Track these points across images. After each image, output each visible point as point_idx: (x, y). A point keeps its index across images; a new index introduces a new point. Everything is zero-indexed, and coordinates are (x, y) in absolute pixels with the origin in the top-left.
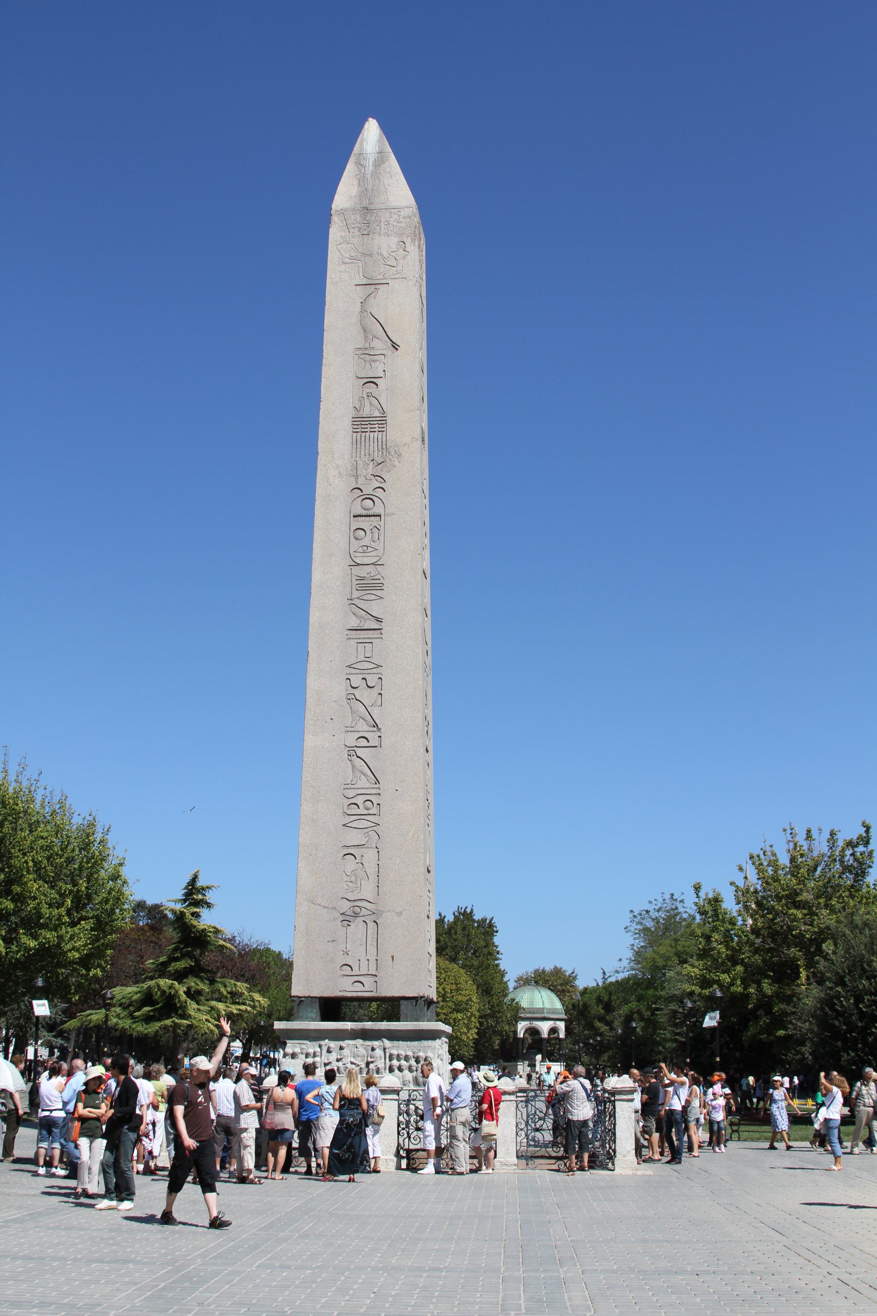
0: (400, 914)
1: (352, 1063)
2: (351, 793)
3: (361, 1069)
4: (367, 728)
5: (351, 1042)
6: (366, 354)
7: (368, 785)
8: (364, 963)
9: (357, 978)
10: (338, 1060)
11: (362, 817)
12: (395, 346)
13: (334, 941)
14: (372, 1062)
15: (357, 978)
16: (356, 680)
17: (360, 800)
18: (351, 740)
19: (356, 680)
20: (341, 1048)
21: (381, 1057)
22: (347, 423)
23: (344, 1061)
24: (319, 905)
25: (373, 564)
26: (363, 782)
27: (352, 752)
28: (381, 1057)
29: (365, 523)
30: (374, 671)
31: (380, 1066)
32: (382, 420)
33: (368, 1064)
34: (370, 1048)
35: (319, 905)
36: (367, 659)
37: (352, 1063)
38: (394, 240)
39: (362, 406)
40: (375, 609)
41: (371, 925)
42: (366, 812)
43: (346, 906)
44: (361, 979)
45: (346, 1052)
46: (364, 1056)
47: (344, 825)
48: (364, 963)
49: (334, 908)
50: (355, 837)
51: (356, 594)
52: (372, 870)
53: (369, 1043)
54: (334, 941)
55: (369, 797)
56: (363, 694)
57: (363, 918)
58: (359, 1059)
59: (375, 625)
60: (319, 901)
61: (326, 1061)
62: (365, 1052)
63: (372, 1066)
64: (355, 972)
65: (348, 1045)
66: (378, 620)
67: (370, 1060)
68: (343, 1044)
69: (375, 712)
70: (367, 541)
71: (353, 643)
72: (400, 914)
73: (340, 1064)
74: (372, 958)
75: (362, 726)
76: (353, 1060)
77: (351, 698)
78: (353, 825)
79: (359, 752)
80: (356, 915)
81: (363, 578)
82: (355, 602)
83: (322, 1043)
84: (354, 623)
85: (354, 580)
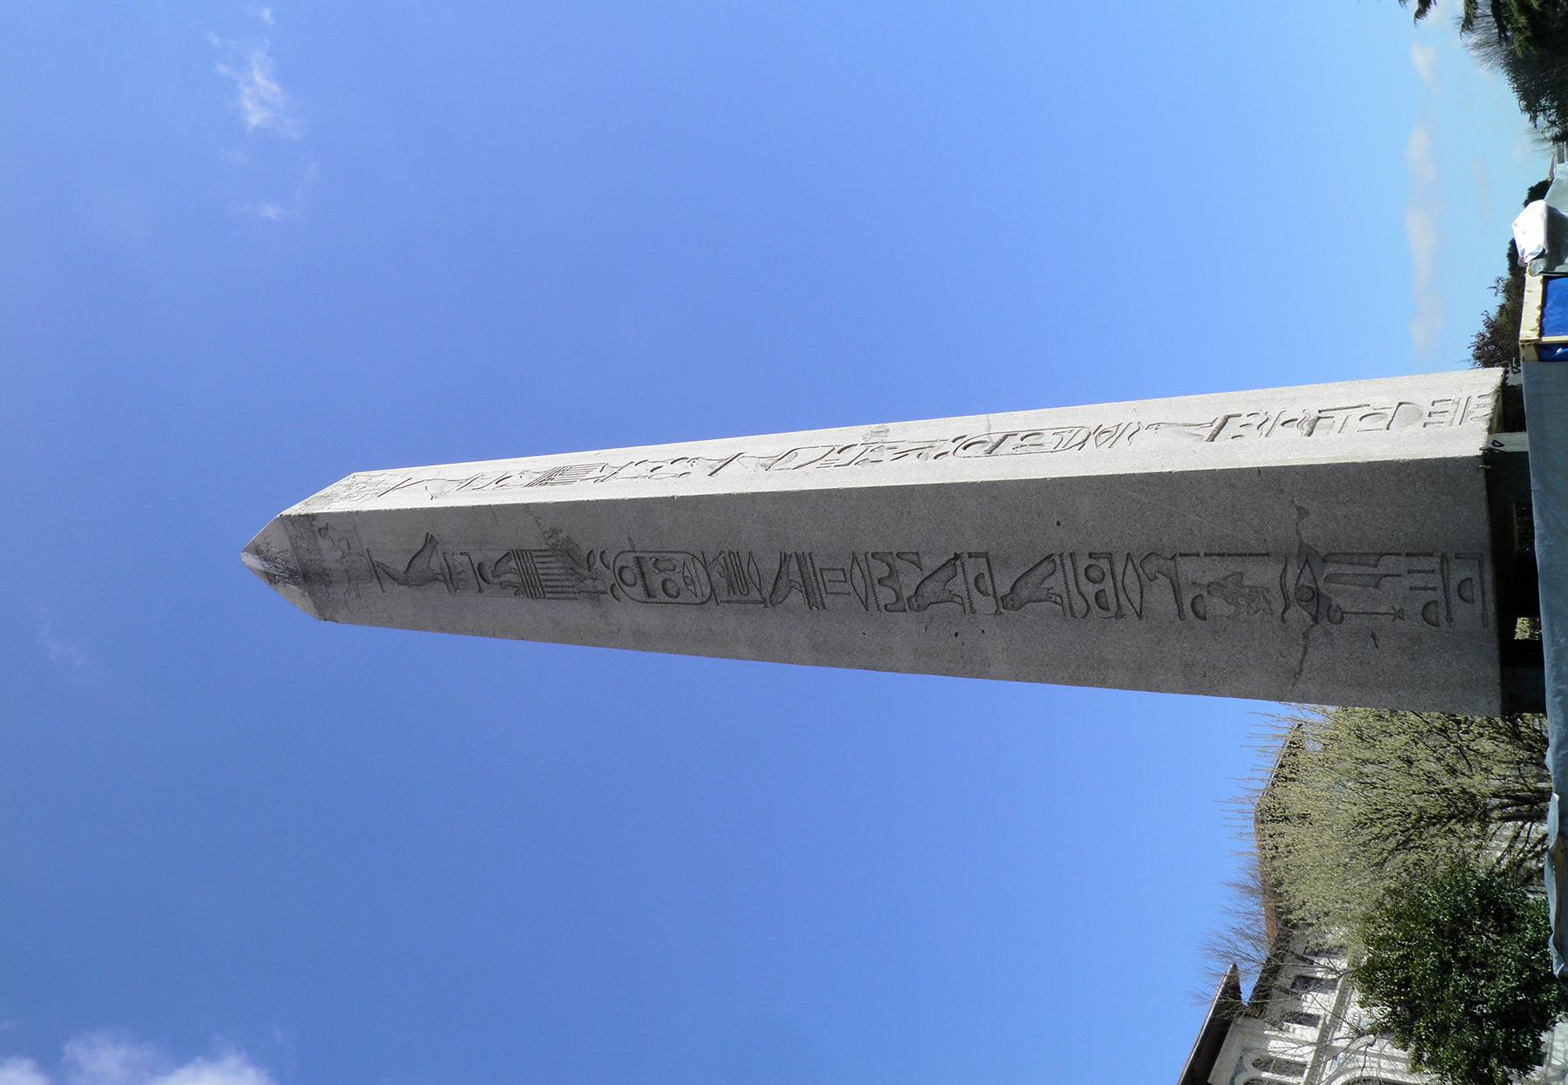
0: (1303, 513)
2: (1079, 605)
4: (960, 577)
6: (450, 578)
7: (1059, 574)
8: (1418, 580)
9: (1453, 594)
11: (1119, 585)
12: (429, 539)
13: (1373, 636)
15: (1453, 594)
16: (886, 595)
17: (1090, 589)
18: (984, 604)
19: (886, 595)
22: (536, 605)
24: (1301, 663)
25: (705, 567)
26: (1056, 583)
29: (656, 581)
30: (864, 566)
32: (518, 554)
35: (1301, 663)
36: (848, 577)
38: (324, 544)
41: (1331, 568)
42: (1109, 578)
43: (1298, 614)
44: (1454, 584)
47: (1140, 616)
48: (1418, 580)
49: (1305, 636)
50: (1161, 598)
51: (755, 595)
52: (1219, 569)
54: (1373, 636)
55: (1081, 571)
57: (1320, 583)
59: (794, 566)
60: (1294, 662)
64: (1439, 595)
66: (784, 560)
69: (930, 563)
71: (828, 600)
72: (1303, 513)
74: (1404, 564)
75: (958, 585)
78: (1136, 598)
79: (1003, 589)
80: (1316, 595)
81: (730, 584)
82: (766, 594)
84: (796, 598)
85: (735, 598)
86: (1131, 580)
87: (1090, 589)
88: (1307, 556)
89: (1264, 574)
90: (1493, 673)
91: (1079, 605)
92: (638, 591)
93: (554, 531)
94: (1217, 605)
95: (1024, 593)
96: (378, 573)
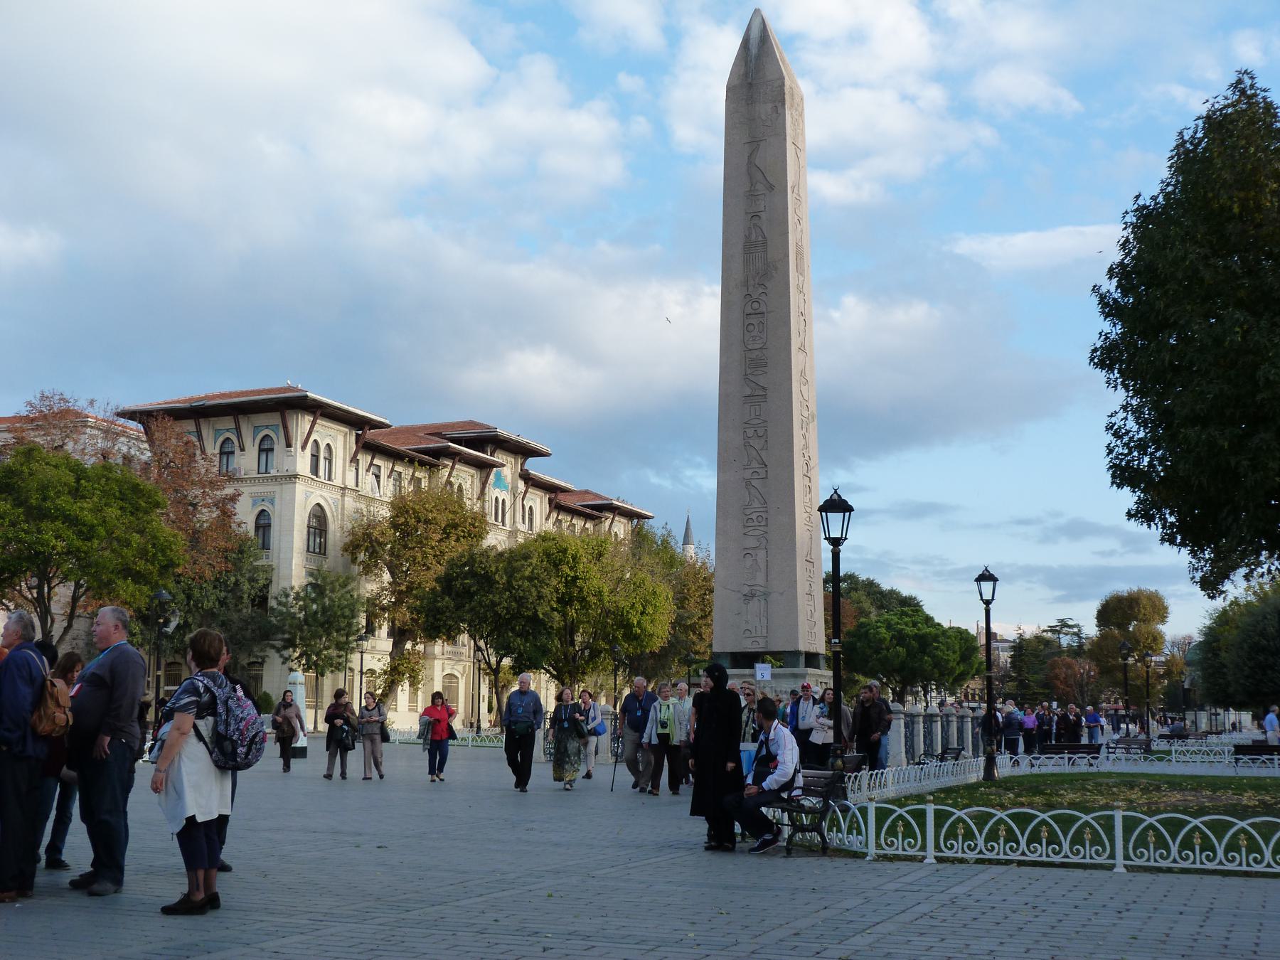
0: (782, 594)
6: (752, 195)
16: (750, 432)
17: (754, 516)
18: (748, 474)
26: (756, 504)
27: (748, 483)
29: (754, 320)
32: (765, 243)
38: (770, 106)
39: (750, 234)
40: (762, 381)
43: (746, 590)
50: (751, 542)
51: (749, 371)
52: (763, 566)
56: (757, 444)
66: (764, 388)
69: (763, 454)
70: (755, 333)
71: (747, 406)
75: (755, 464)
77: (747, 445)
79: (754, 482)
80: (753, 596)
84: (748, 391)
86: (757, 533)
87: (754, 516)
88: (766, 595)
89: (760, 579)
90: (728, 650)
91: (748, 512)
92: (749, 310)
93: (776, 269)
94: (749, 561)
95: (753, 490)
96: (755, 143)
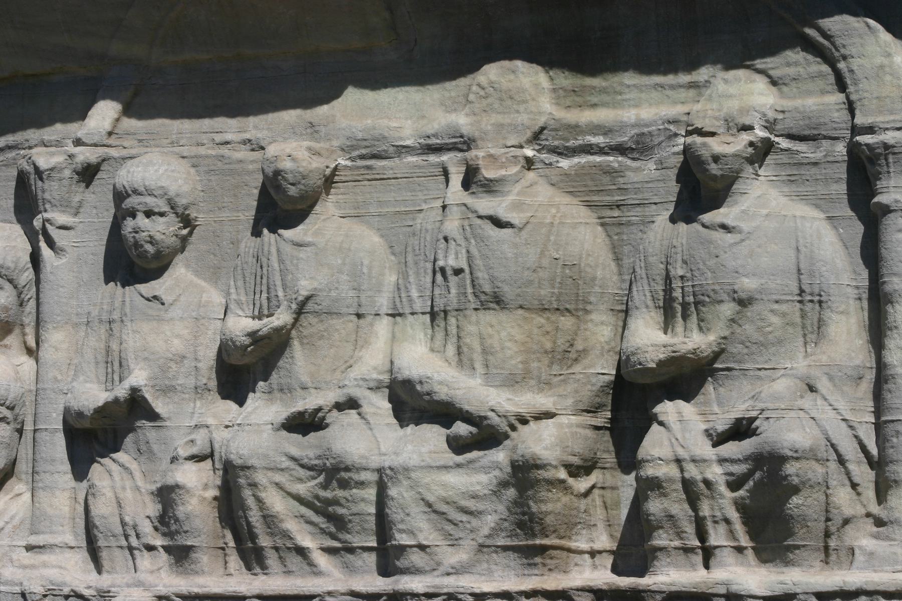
1: (412, 404)
3: (524, 475)
5: (401, 112)
10: (240, 372)
14: (685, 378)
20: (280, 206)
21: (811, 301)
23: (309, 378)
28: (811, 301)
31: (789, 432)
33: (632, 400)
34: (655, 177)
37: (412, 404)
45: (336, 244)
46: (567, 300)
53: (641, 103)
58: (505, 332)
61: (92, 395)
62: (584, 237)
63: (680, 432)
65: (372, 152)
67: (650, 339)
68: (289, 140)
73: (253, 427)
76: (422, 359)
83: (50, 149)
